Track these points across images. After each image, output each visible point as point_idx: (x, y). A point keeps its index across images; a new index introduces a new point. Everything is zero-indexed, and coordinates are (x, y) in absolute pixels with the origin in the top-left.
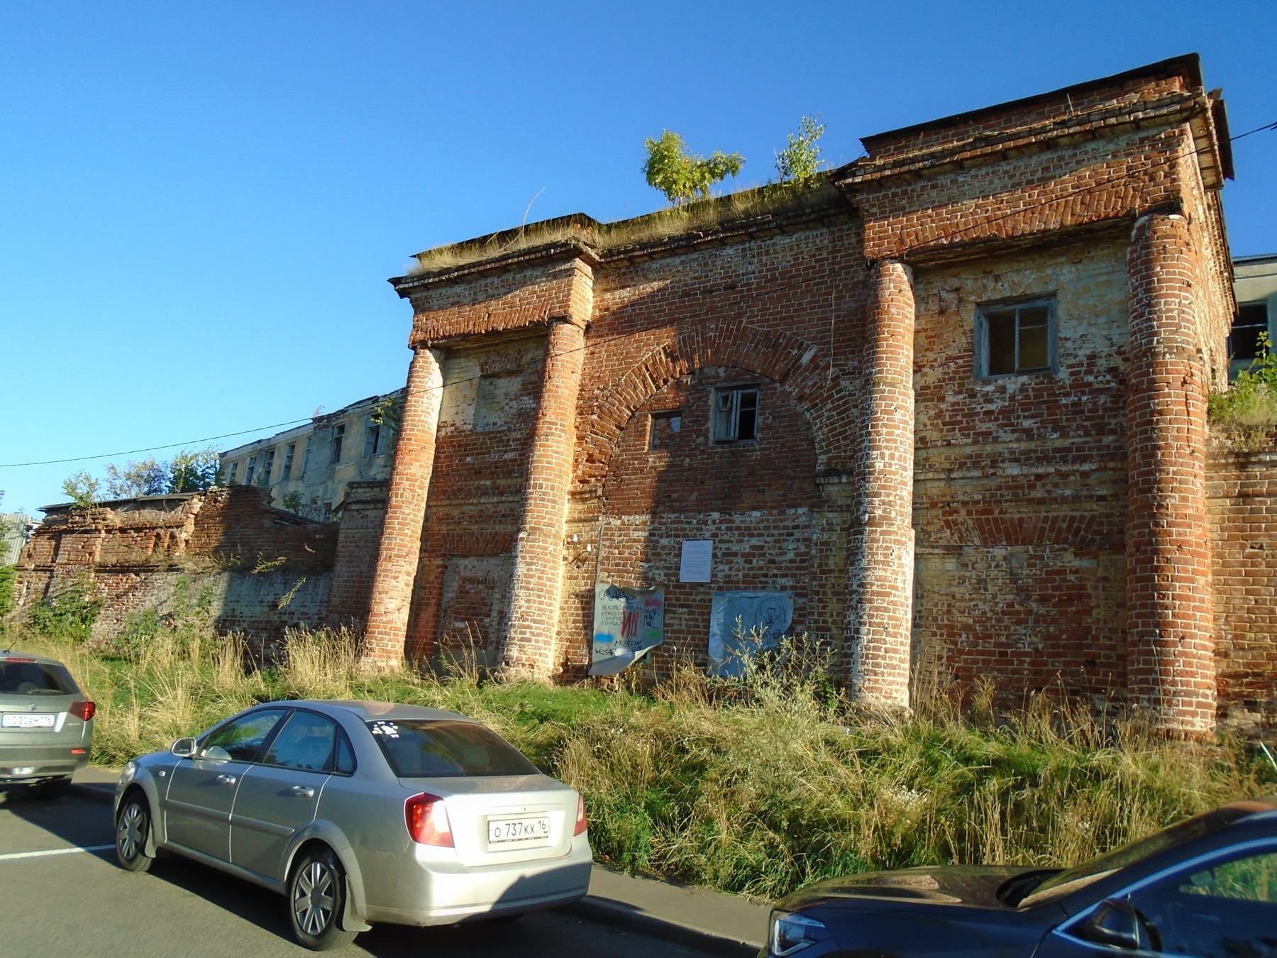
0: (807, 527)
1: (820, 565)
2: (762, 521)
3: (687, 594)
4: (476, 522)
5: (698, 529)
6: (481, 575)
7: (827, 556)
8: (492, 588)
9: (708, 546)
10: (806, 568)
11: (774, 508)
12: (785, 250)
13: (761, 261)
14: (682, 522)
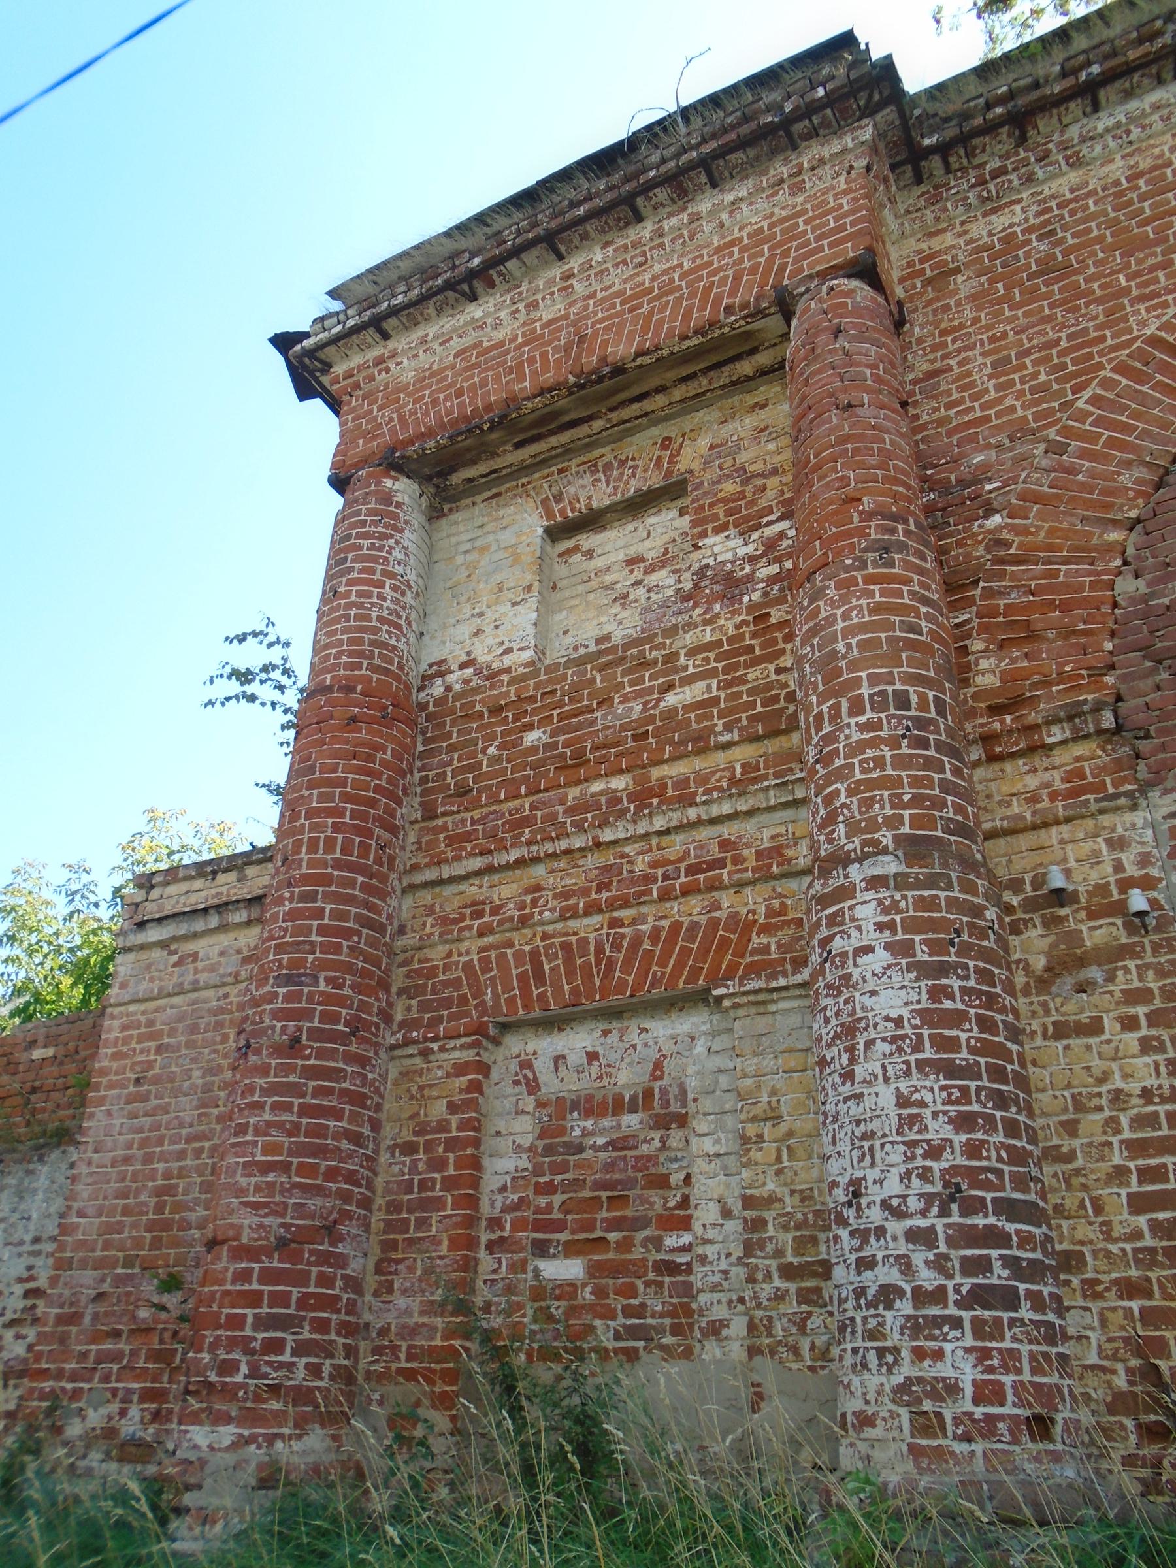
4: (592, 908)
6: (628, 1077)
8: (682, 1121)
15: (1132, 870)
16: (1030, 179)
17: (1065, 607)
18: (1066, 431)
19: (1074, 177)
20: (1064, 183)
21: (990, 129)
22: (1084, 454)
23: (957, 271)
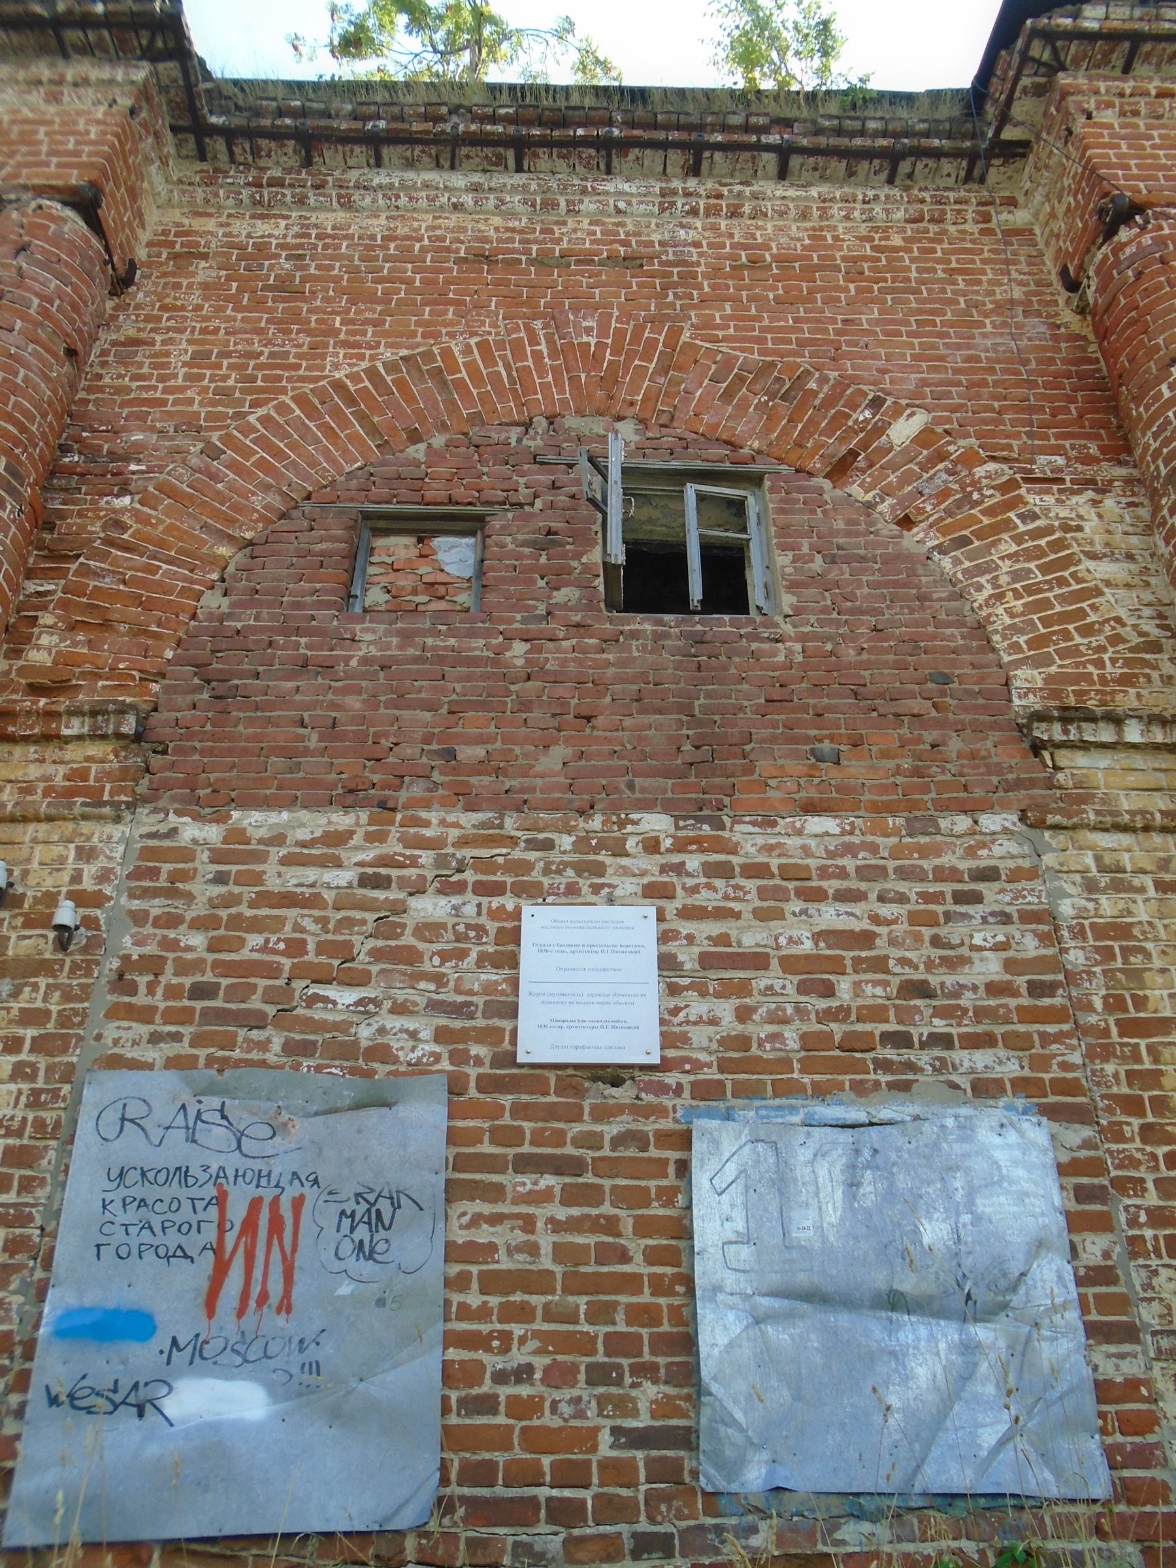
0: (1032, 874)
1: (1114, 1004)
2: (850, 850)
3: (552, 1112)
5: (581, 869)
7: (1136, 975)
9: (636, 925)
10: (1057, 1015)
11: (890, 809)
12: (785, 213)
13: (715, 228)
14: (513, 841)
15: (88, 884)
16: (301, 201)
17: (138, 601)
18: (228, 440)
19: (341, 216)
20: (328, 219)
21: (277, 135)
22: (233, 466)
23: (205, 257)
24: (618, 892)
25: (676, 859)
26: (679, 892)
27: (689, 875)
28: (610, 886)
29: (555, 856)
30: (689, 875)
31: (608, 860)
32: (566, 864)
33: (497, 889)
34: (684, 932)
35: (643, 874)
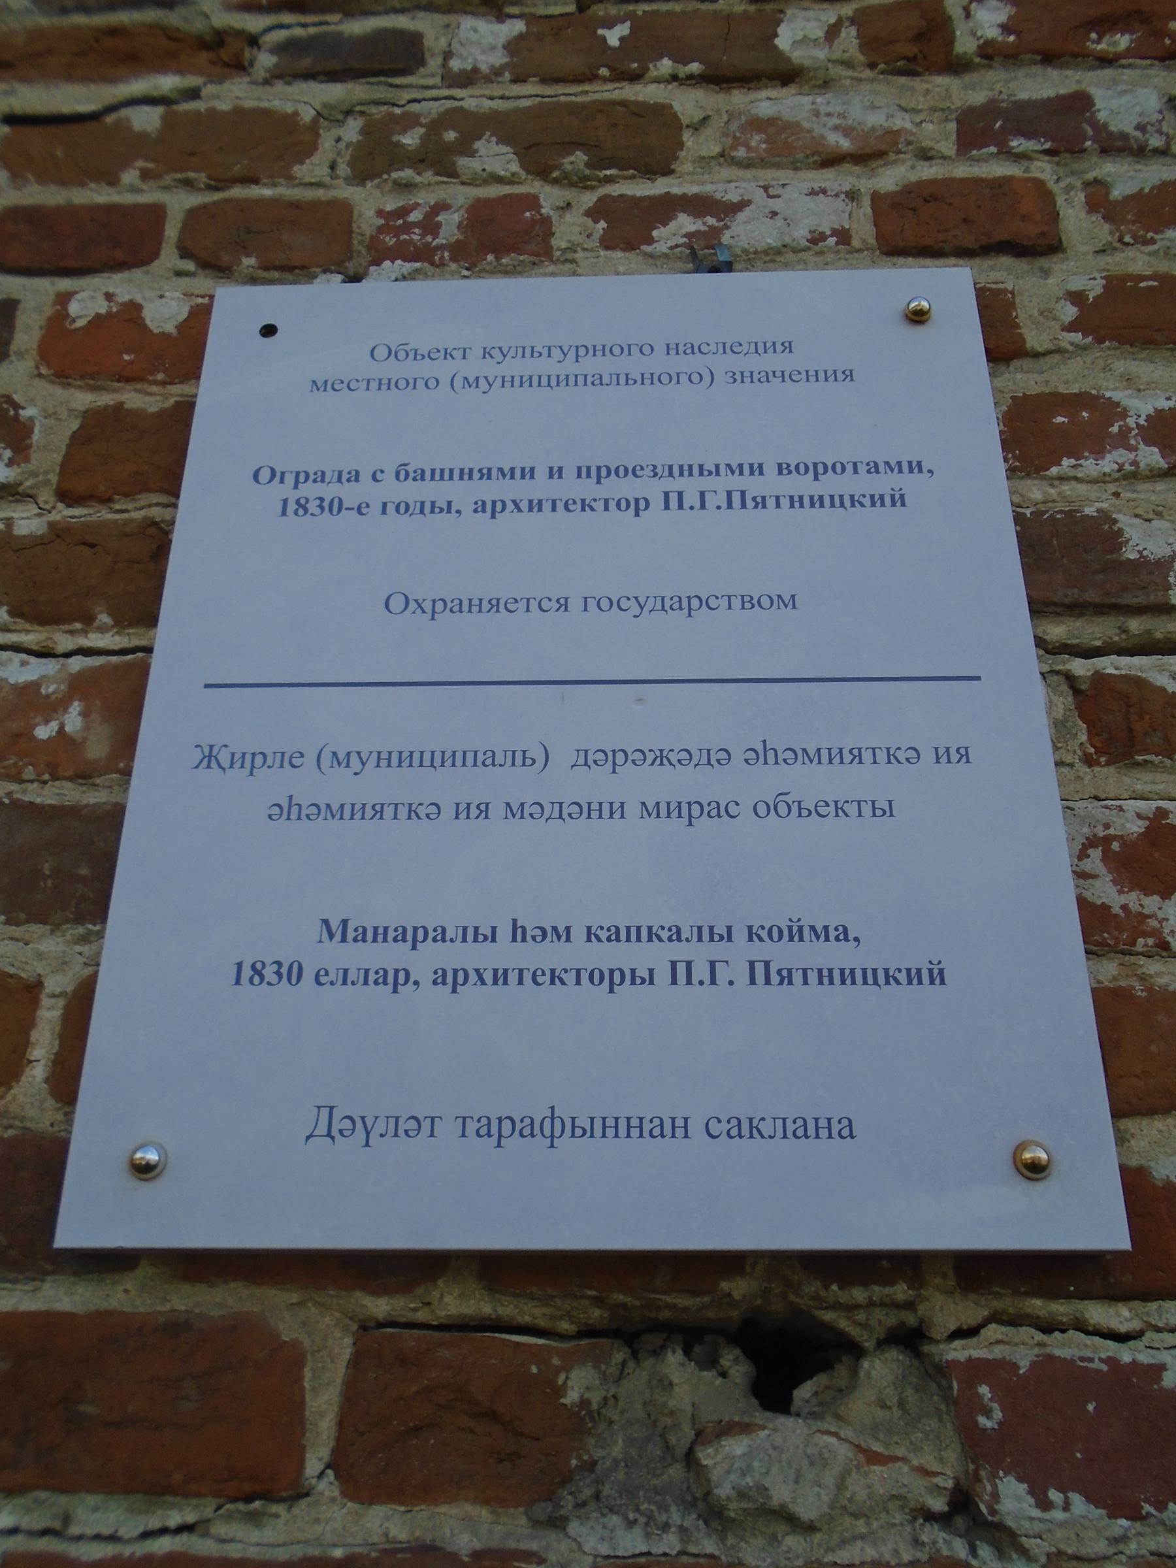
5: (540, 144)
24: (744, 232)
25: (1040, 85)
26: (1074, 218)
27: (1115, 146)
28: (698, 205)
29: (422, 96)
30: (1115, 146)
31: (688, 103)
32: (473, 128)
33: (125, 241)
34: (1141, 407)
35: (867, 156)
